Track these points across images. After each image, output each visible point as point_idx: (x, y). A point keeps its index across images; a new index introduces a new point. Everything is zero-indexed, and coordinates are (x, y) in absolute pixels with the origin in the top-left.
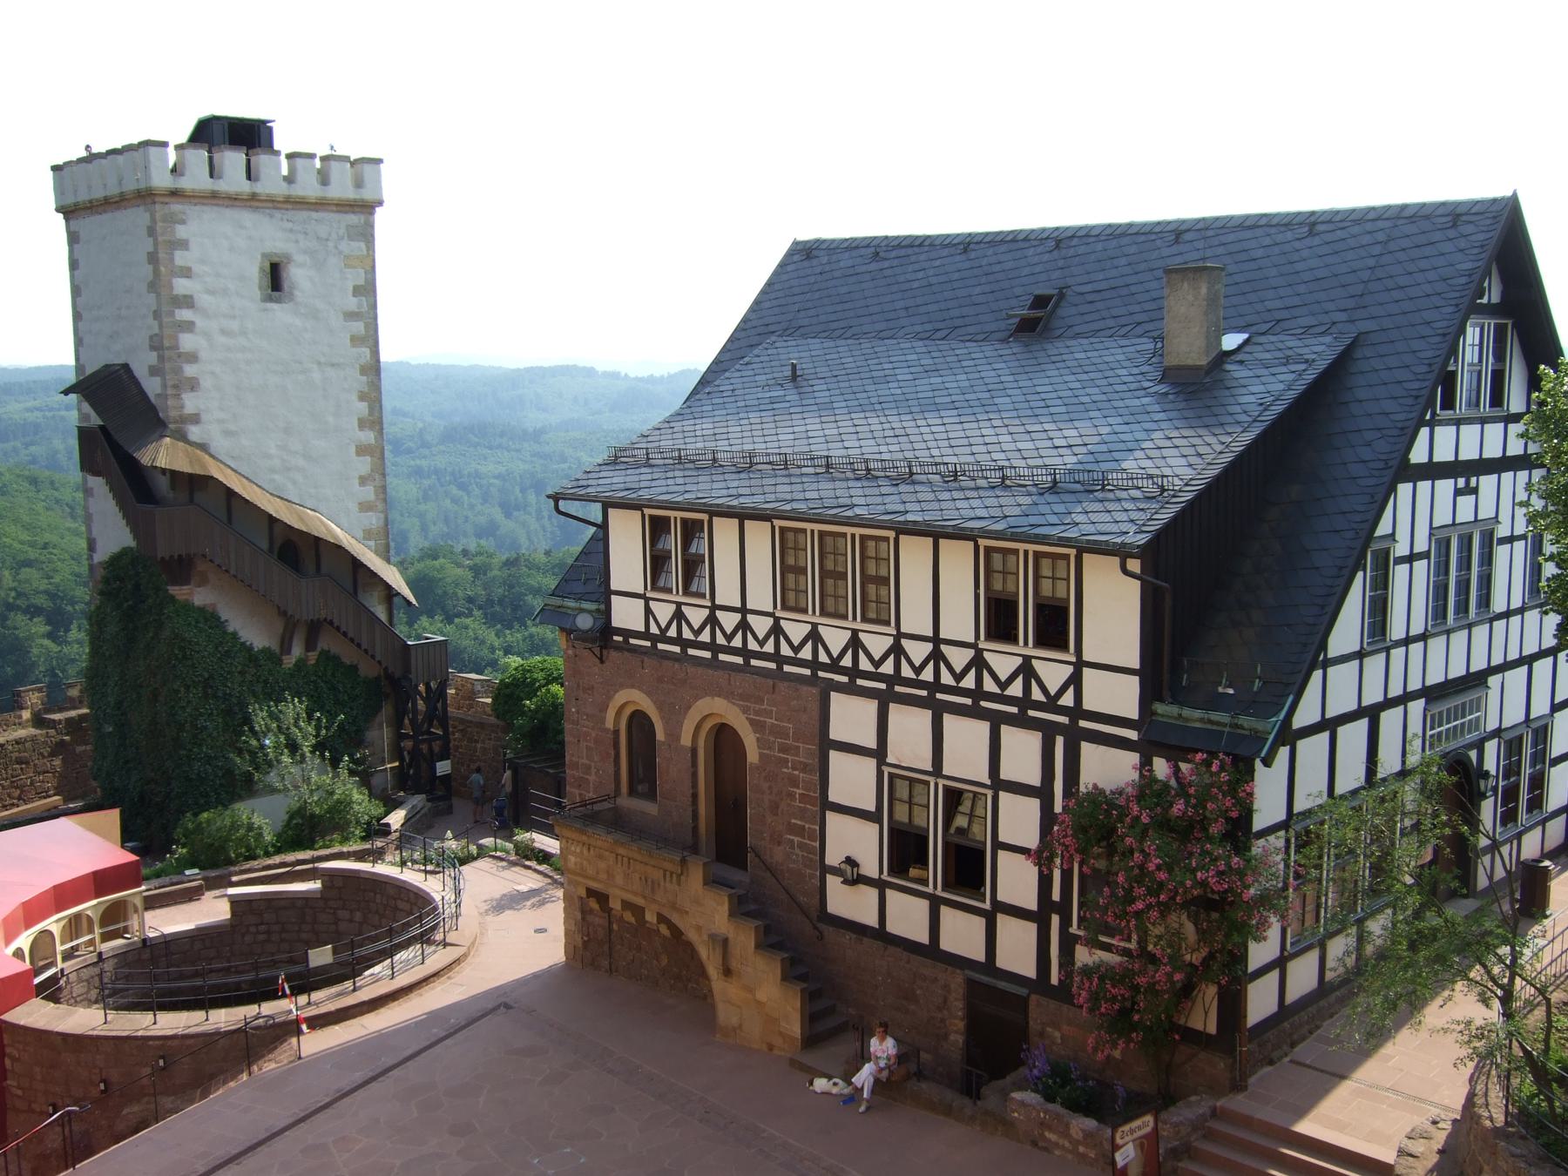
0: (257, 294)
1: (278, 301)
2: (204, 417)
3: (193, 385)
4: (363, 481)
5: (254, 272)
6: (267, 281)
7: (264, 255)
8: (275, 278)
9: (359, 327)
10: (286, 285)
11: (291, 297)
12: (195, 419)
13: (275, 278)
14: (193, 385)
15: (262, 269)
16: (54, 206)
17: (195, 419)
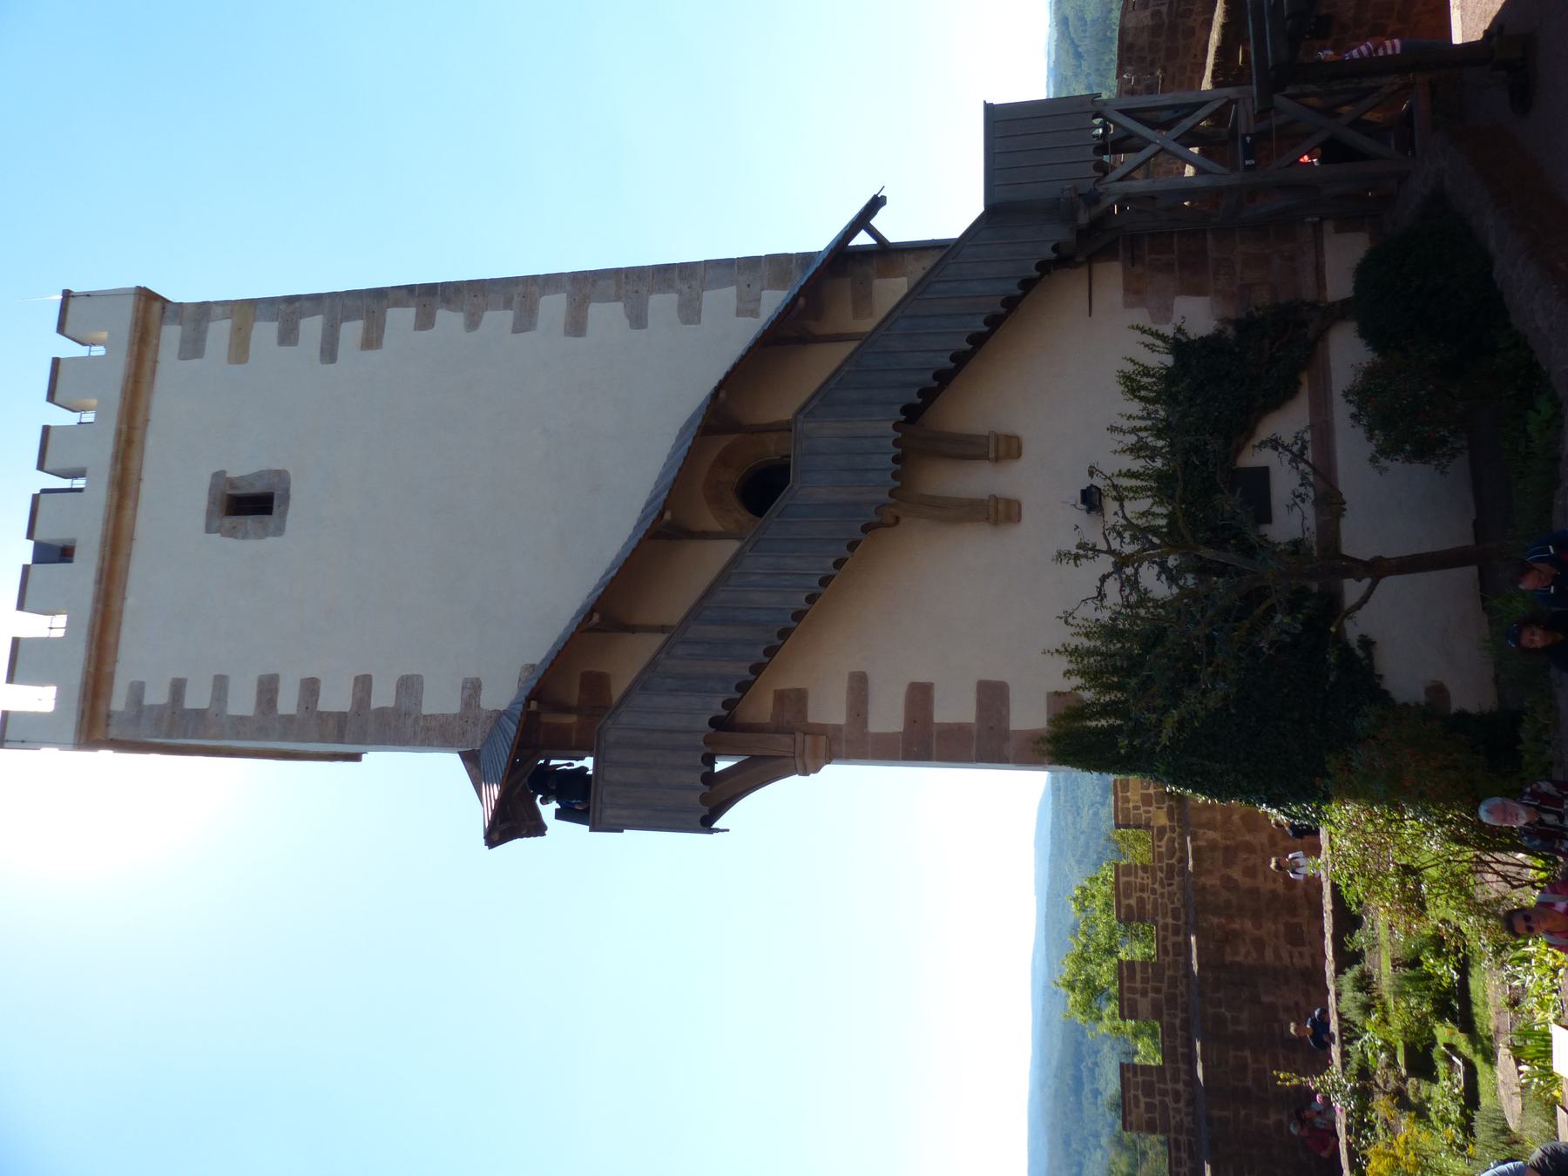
0: (270, 541)
1: (286, 498)
2: (472, 673)
3: (409, 686)
4: (638, 319)
5: (248, 550)
6: (250, 521)
7: (208, 530)
8: (249, 505)
9: (351, 331)
10: (258, 488)
11: (282, 475)
12: (473, 688)
13: (249, 505)
14: (409, 686)
15: (231, 533)
17: (473, 688)
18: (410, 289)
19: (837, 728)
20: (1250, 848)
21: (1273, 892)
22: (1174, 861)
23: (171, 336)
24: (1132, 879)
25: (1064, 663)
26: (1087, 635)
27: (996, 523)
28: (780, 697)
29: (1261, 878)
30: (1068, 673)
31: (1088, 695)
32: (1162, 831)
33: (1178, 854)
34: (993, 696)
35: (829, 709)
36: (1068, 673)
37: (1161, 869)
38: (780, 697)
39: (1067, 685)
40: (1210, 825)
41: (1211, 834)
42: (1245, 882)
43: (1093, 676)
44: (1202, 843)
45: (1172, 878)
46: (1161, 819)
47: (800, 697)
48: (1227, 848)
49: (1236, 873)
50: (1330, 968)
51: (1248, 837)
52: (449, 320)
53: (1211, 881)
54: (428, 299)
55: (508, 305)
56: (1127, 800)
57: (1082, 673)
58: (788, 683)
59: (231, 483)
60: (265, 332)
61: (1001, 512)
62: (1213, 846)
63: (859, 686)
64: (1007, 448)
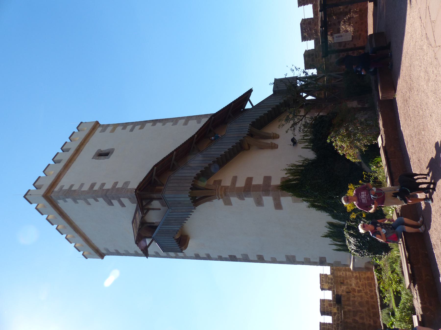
10: (107, 152)
16: (100, 260)
18: (153, 120)
19: (228, 186)
20: (361, 312)
21: (370, 324)
22: (339, 322)
23: (100, 129)
24: (325, 326)
25: (286, 172)
26: (292, 167)
27: (272, 149)
28: (215, 181)
29: (365, 320)
30: (286, 174)
31: (291, 178)
32: (335, 314)
33: (340, 320)
34: (267, 179)
35: (227, 182)
36: (286, 174)
37: (335, 324)
38: (215, 181)
39: (286, 176)
40: (348, 305)
41: (349, 308)
42: (360, 321)
43: (292, 174)
44: (346, 310)
45: (338, 327)
46: (335, 310)
47: (220, 181)
48: (354, 312)
49: (357, 318)
50: (380, 310)
51: (361, 309)
52: (159, 125)
53: (350, 320)
54: (155, 122)
55: (172, 122)
56: (324, 305)
57: (289, 173)
58: (217, 179)
59: (101, 151)
60: (120, 128)
61: (274, 147)
62: (349, 311)
63: (235, 179)
64: (276, 137)
